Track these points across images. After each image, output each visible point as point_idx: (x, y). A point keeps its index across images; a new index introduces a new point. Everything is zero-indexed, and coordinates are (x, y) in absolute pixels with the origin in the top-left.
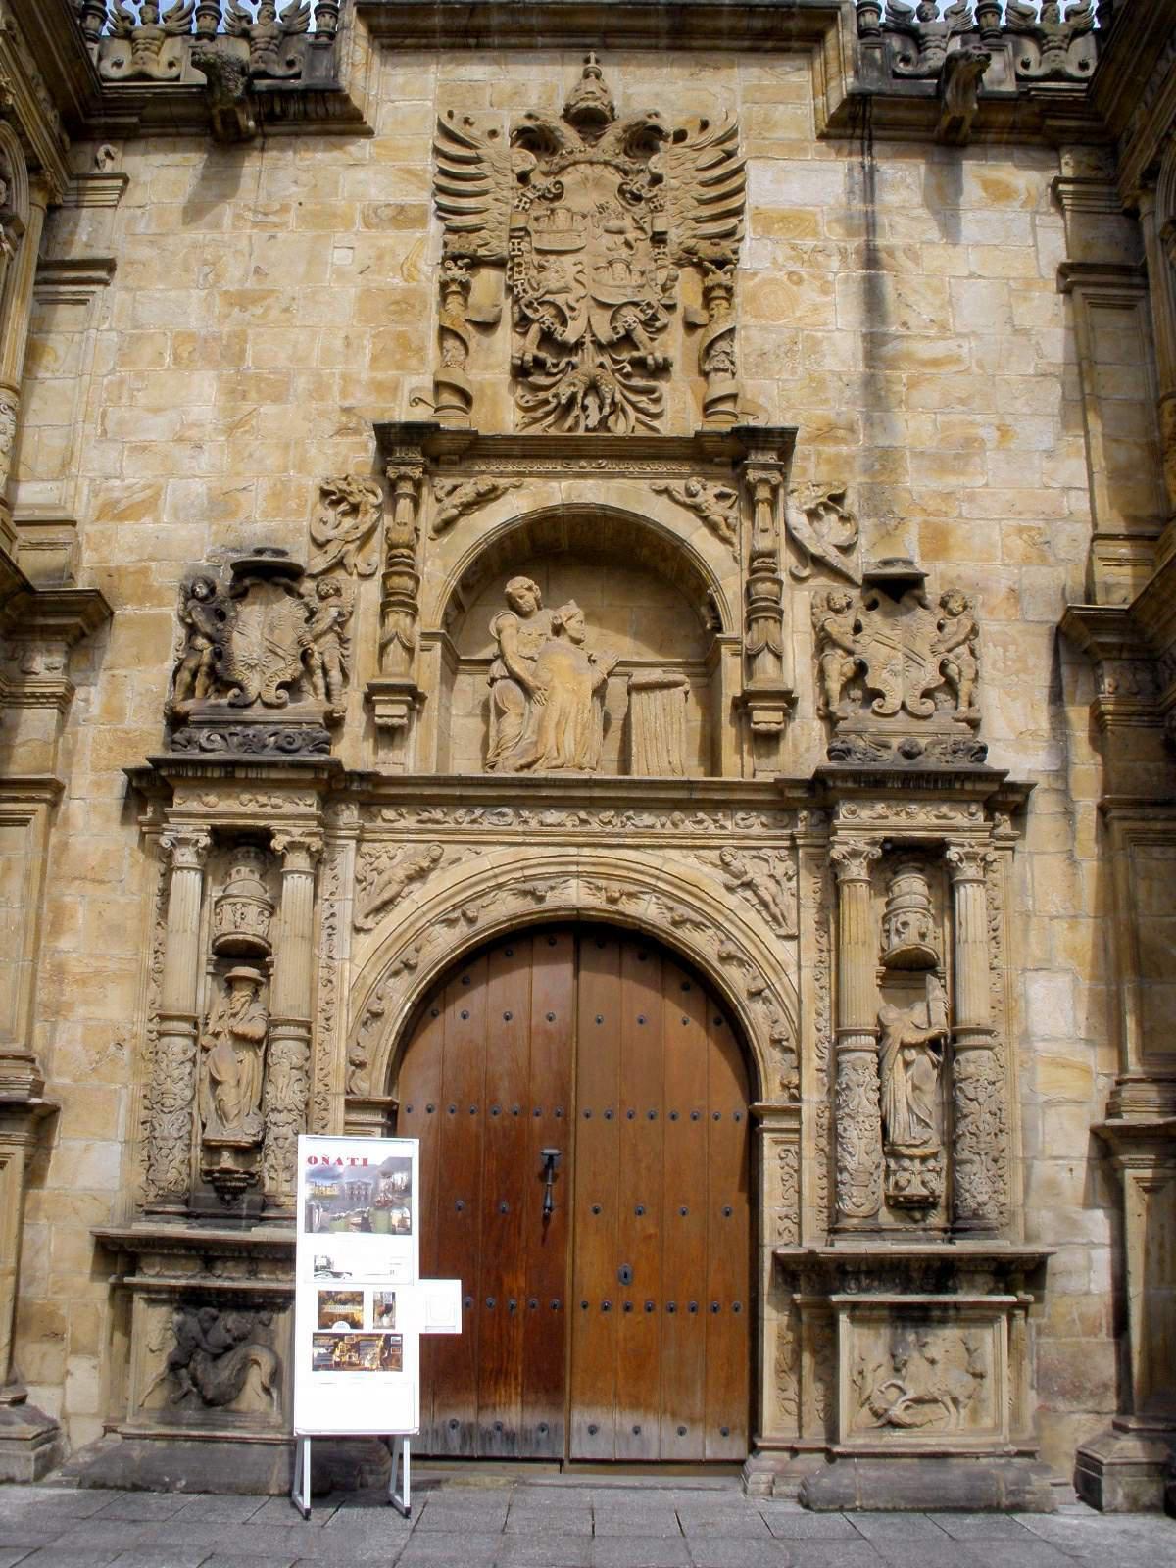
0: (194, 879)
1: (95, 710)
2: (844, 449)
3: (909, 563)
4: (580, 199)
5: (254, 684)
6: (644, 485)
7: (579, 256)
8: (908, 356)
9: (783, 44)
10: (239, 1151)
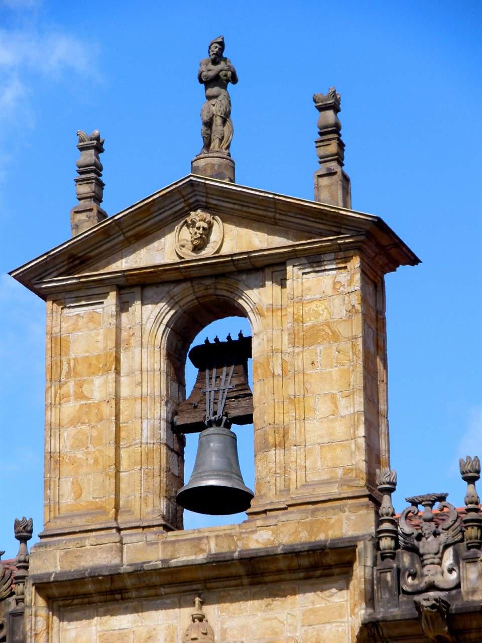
9: (327, 572)
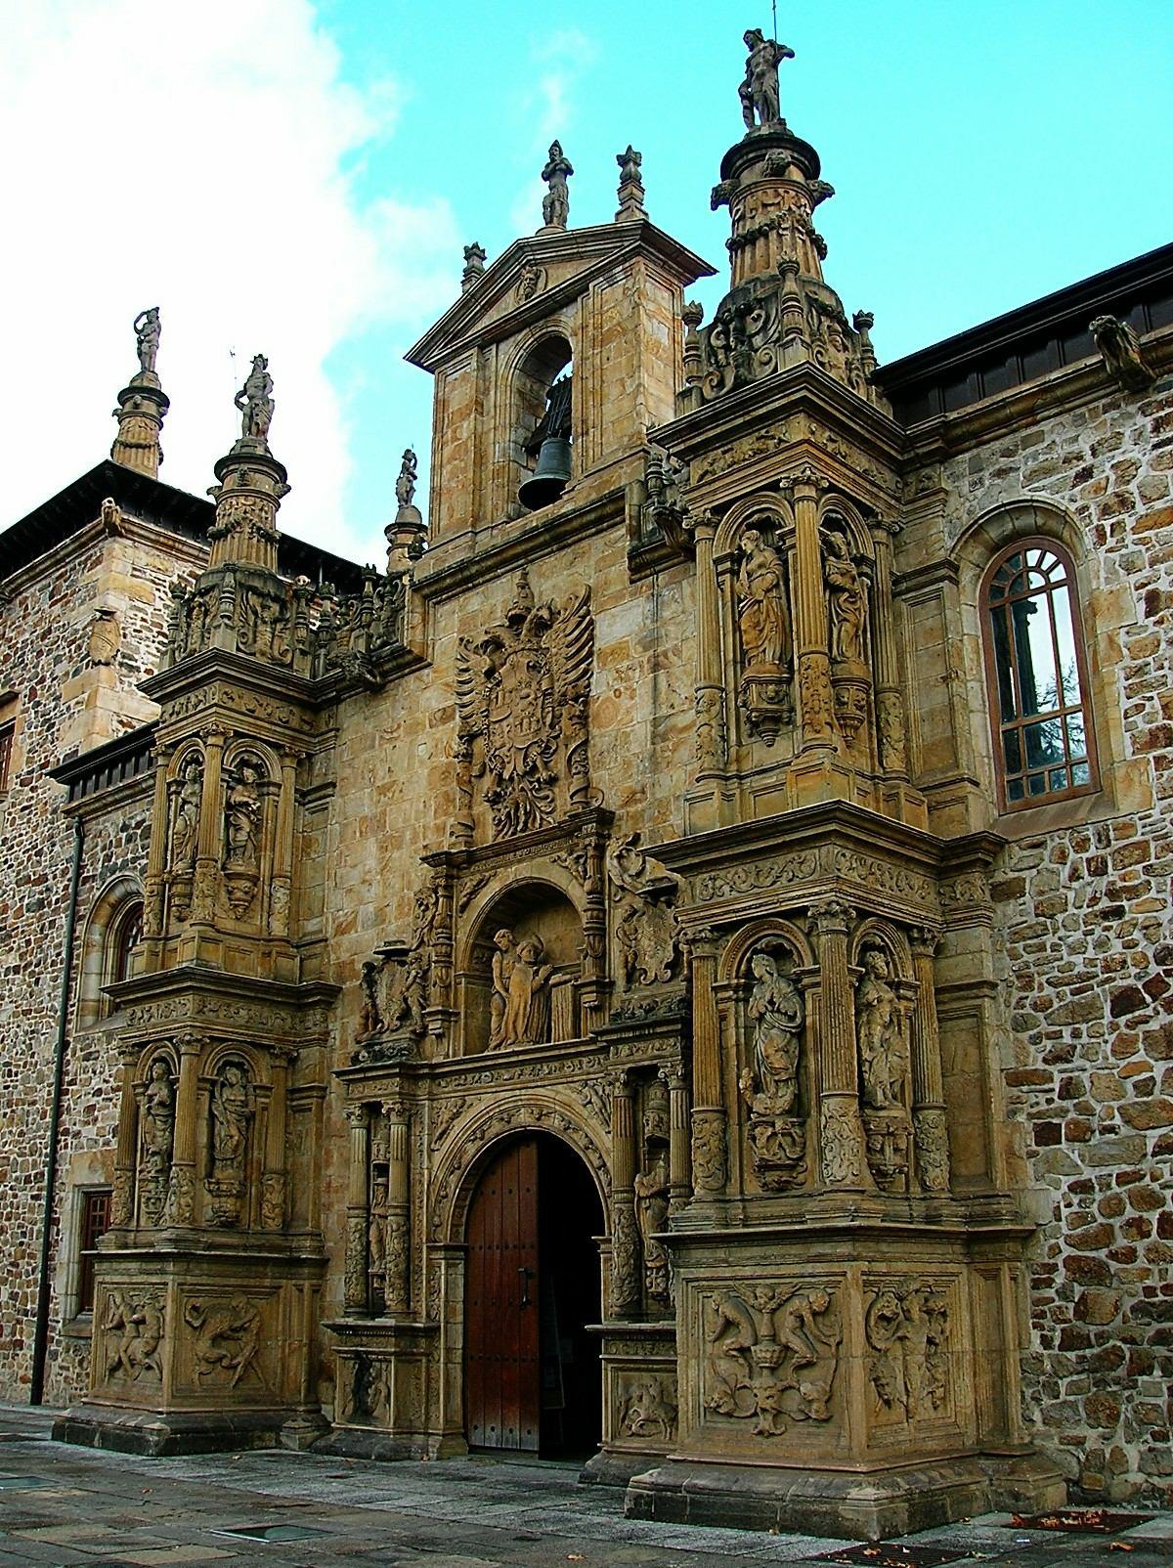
4: (509, 683)
6: (547, 859)
7: (511, 720)
8: (673, 728)
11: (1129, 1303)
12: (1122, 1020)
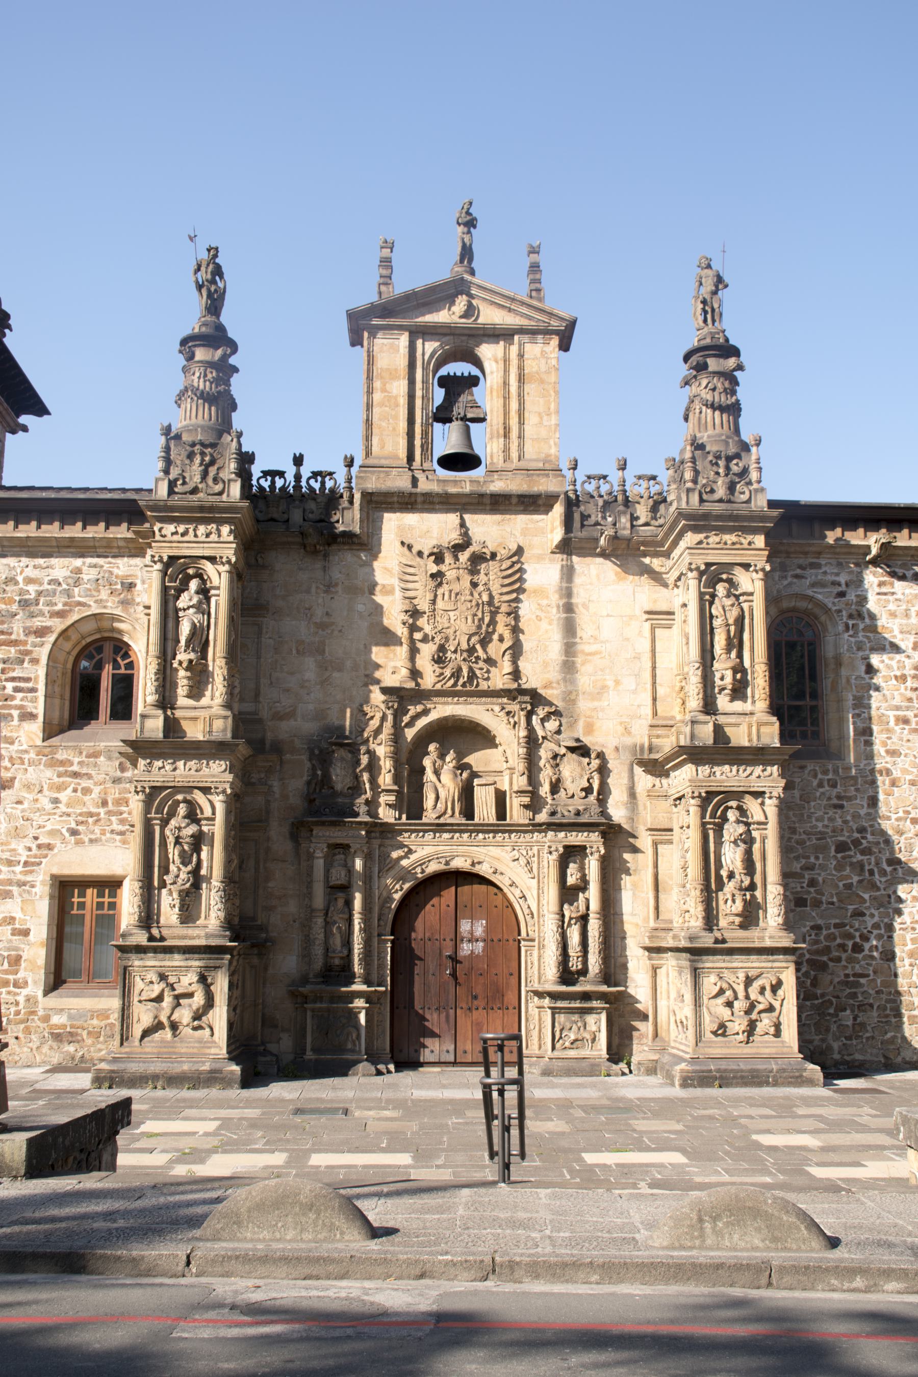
0: (321, 861)
1: (277, 796)
2: (555, 692)
3: (578, 740)
5: (339, 787)
8: (583, 652)
10: (342, 958)
11: (836, 980)
12: (839, 855)
